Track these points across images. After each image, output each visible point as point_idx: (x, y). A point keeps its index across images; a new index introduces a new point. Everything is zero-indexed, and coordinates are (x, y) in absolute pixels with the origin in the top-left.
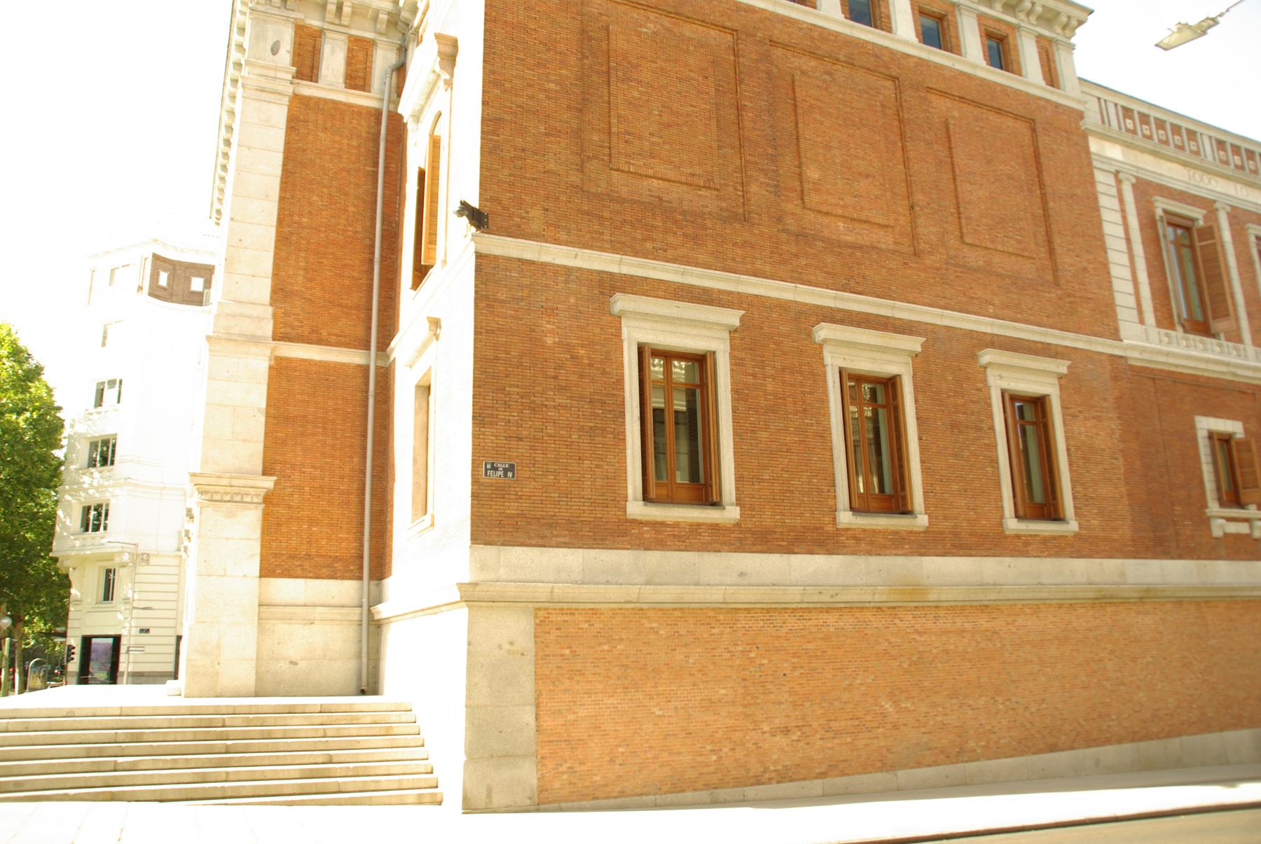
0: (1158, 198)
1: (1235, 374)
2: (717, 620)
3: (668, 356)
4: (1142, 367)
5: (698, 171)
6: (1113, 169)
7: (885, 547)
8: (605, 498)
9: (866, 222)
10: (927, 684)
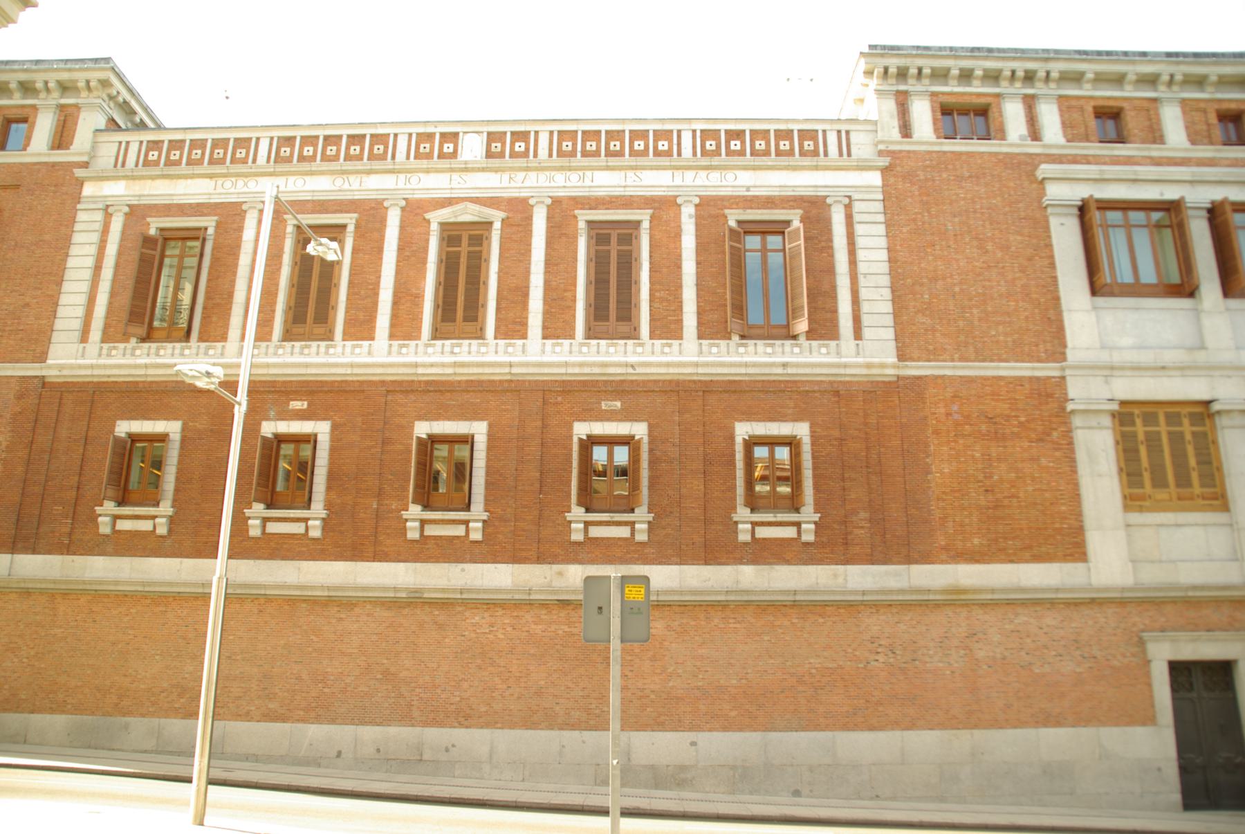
4: (64, 382)
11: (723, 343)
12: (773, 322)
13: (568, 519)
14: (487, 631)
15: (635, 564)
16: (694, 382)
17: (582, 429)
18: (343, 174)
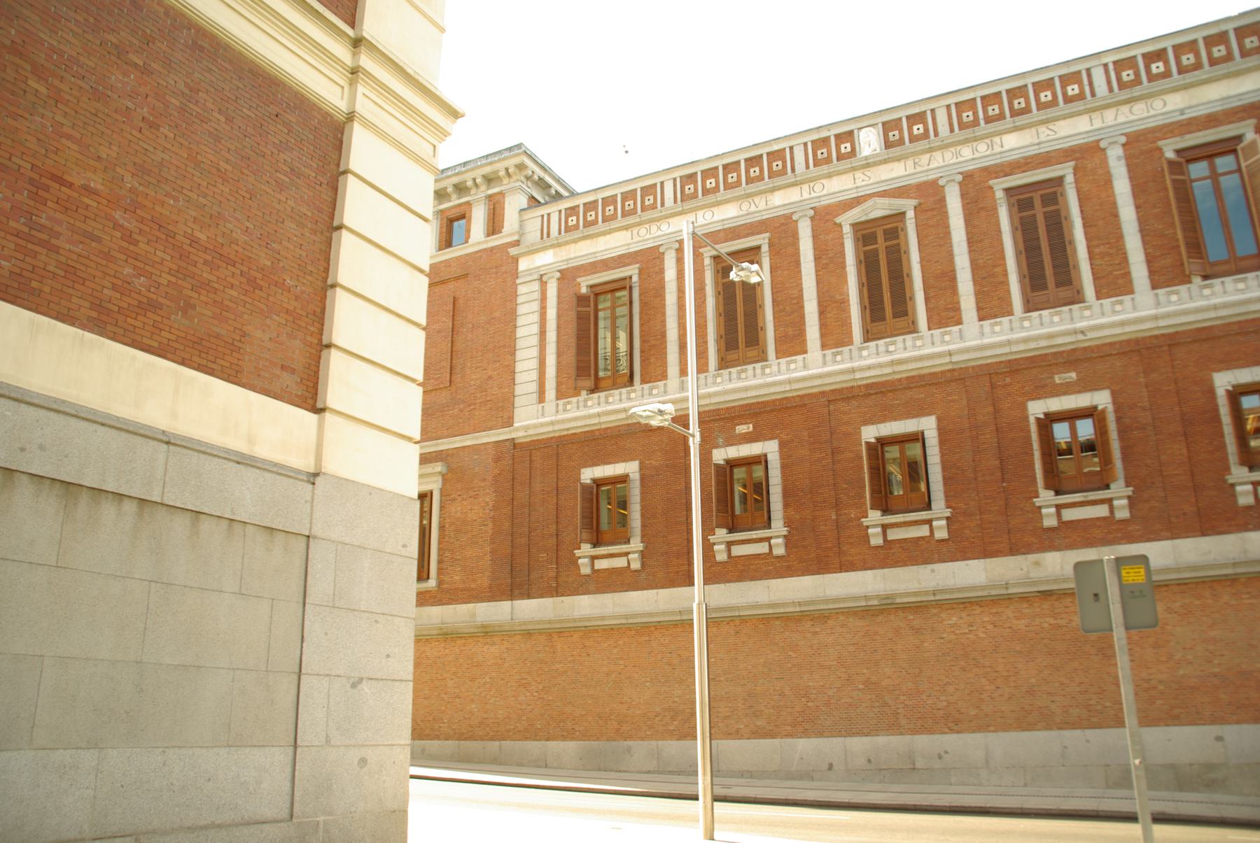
6: (536, 277)
11: (1183, 289)
12: (1240, 253)
13: (1037, 504)
14: (967, 631)
15: (1120, 544)
16: (1156, 337)
17: (1037, 409)
18: (747, 197)
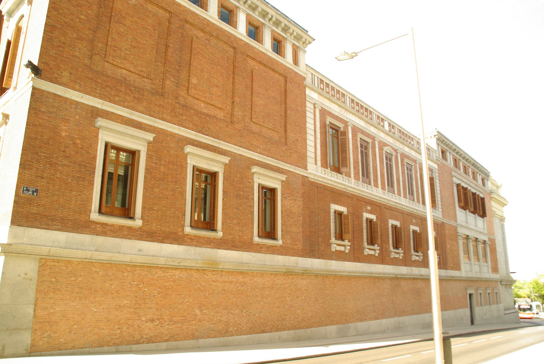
0: (328, 117)
1: (346, 189)
2: (126, 270)
3: (119, 149)
4: (314, 182)
5: (144, 69)
6: (313, 102)
7: (203, 244)
8: (81, 210)
9: (213, 105)
10: (215, 303)
